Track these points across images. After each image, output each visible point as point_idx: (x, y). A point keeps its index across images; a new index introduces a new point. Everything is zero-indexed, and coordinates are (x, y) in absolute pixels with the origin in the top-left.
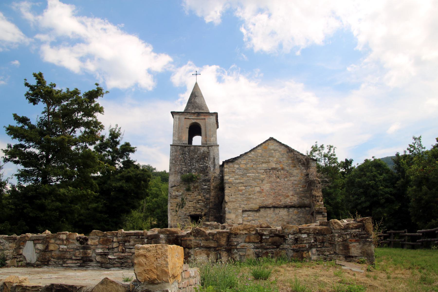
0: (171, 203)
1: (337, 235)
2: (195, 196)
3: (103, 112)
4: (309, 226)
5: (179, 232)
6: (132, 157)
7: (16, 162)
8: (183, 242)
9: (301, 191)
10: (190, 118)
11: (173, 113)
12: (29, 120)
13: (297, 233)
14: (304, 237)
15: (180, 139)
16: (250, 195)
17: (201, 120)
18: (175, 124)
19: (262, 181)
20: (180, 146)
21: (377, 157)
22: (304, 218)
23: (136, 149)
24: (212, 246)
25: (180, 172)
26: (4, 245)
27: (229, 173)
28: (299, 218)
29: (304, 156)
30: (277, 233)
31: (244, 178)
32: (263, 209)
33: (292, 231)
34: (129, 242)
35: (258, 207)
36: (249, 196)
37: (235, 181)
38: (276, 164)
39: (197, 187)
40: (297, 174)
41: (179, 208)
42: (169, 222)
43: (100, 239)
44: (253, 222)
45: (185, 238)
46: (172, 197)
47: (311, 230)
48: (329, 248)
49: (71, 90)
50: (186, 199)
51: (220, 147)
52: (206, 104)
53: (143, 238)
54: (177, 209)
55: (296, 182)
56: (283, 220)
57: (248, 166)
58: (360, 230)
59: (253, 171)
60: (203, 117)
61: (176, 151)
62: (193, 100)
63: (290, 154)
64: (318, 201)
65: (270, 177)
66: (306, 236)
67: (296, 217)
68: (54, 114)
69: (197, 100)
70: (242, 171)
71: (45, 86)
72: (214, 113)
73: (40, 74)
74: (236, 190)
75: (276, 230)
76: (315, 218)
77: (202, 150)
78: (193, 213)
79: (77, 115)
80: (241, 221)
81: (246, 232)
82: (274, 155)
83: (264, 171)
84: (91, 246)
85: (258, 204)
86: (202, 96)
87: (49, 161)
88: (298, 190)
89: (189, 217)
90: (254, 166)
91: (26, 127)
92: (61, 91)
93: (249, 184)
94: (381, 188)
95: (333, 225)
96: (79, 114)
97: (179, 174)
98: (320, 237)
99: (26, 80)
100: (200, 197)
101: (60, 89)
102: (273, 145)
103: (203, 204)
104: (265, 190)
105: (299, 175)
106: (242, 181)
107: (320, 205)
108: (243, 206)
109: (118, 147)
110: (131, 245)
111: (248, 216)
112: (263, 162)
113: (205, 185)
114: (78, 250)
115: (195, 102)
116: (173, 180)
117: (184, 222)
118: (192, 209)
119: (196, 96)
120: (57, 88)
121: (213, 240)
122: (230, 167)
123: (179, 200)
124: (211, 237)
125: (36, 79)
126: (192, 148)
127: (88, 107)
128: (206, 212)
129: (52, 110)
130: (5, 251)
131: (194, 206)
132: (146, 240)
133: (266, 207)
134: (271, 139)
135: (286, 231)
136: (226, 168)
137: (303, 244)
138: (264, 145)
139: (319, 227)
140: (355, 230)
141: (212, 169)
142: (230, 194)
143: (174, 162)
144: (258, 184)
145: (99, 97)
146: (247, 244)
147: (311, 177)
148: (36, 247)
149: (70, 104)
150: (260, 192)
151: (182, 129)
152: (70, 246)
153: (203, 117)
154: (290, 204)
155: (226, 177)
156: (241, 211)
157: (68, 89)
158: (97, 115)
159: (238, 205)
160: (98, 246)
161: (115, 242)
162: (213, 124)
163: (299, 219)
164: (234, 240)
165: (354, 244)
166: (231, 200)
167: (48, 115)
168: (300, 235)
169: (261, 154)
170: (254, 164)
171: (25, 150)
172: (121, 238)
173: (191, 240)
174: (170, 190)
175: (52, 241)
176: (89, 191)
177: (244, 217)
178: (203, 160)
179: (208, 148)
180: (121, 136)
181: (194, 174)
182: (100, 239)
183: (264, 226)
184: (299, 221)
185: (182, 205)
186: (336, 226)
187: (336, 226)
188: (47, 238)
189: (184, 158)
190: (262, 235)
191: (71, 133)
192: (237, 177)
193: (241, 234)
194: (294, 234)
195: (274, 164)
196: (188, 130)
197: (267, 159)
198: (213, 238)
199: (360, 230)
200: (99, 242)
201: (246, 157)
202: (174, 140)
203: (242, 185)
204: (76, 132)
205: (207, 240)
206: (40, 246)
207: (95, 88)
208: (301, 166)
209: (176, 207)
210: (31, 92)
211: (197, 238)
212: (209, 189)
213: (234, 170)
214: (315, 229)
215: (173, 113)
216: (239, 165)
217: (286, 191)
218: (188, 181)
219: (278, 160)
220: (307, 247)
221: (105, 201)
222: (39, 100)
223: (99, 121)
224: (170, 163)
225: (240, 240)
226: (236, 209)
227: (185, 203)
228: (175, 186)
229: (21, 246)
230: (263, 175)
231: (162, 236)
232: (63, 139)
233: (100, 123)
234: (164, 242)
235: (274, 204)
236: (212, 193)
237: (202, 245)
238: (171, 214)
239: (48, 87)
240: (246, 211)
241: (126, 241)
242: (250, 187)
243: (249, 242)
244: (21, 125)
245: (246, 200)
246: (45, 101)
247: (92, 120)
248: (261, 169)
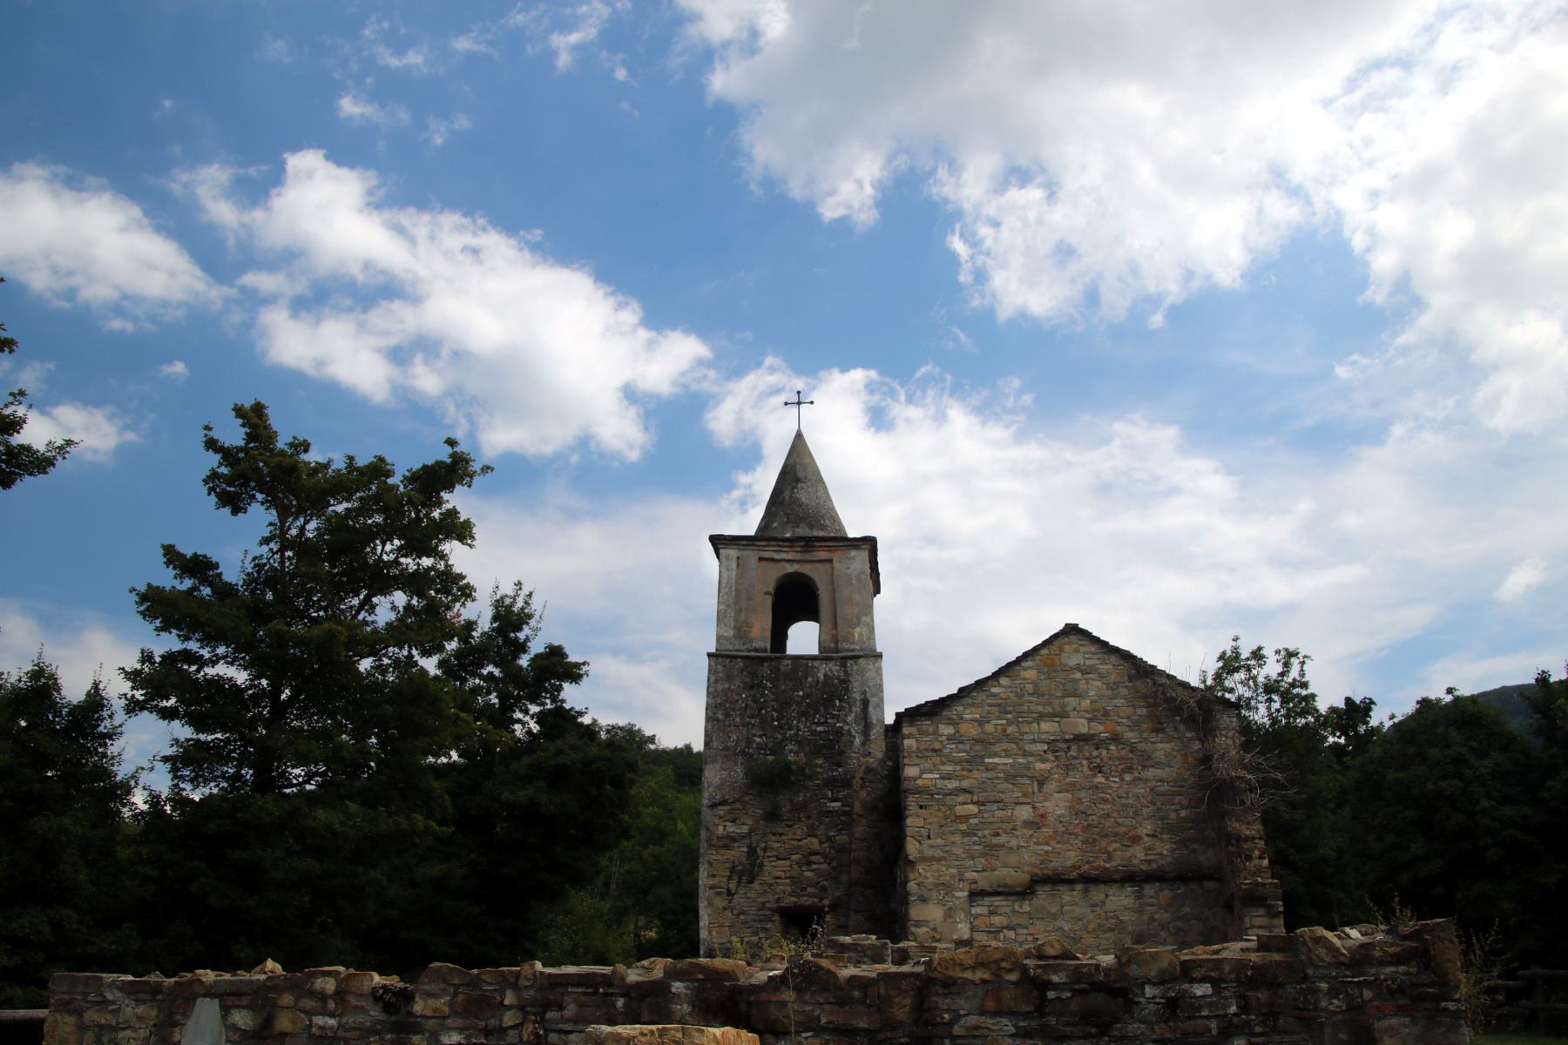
0: (710, 864)
1: (1324, 986)
2: (799, 837)
3: (472, 538)
4: (1217, 952)
5: (740, 975)
6: (572, 696)
7: (168, 714)
8: (754, 1011)
10: (776, 556)
11: (718, 542)
12: (216, 566)
13: (1175, 979)
14: (1199, 993)
15: (741, 632)
17: (819, 566)
18: (725, 581)
19: (1041, 784)
20: (743, 658)
21: (1465, 691)
23: (585, 668)
24: (863, 1025)
25: (743, 753)
26: (117, 1011)
27: (920, 753)
28: (1179, 918)
29: (1195, 689)
30: (1101, 977)
31: (976, 774)
33: (1154, 973)
34: (561, 1008)
35: (1028, 877)
36: (995, 840)
37: (940, 783)
38: (1090, 720)
39: (803, 806)
40: (1168, 755)
41: (739, 882)
42: (703, 934)
43: (456, 994)
44: (1011, 934)
45: (764, 996)
46: (715, 842)
47: (1227, 968)
48: (1295, 1037)
49: (363, 461)
50: (765, 849)
51: (885, 664)
52: (833, 509)
53: (612, 995)
54: (733, 886)
55: (1165, 787)
56: (1120, 927)
57: (989, 728)
58: (1413, 970)
59: (1005, 746)
60: (823, 555)
61: (729, 678)
62: (787, 494)
63: (1139, 684)
64: (1249, 858)
65: (1068, 768)
66: (1210, 991)
67: (1167, 916)
68: (301, 546)
69: (803, 496)
70: (968, 747)
71: (272, 450)
73: (259, 409)
74: (946, 817)
75: (1097, 966)
76: (1241, 918)
77: (823, 670)
78: (789, 901)
79: (379, 548)
80: (963, 931)
81: (986, 976)
82: (1082, 686)
84: (423, 1021)
85: (1027, 868)
86: (820, 481)
87: (279, 709)
88: (1173, 816)
89: (776, 917)
90: (1010, 730)
91: (206, 591)
92: (326, 466)
93: (993, 795)
94: (1486, 804)
95: (1310, 951)
96: (388, 547)
98: (1262, 995)
99: (208, 428)
100: (814, 840)
101: (322, 460)
102: (1076, 651)
103: (824, 866)
104: (1050, 818)
105: (1178, 762)
106: (965, 784)
107: (1258, 869)
108: (970, 875)
109: (524, 661)
110: (568, 1020)
111: (992, 913)
112: (1042, 716)
113: (834, 800)
114: (376, 1032)
115: (797, 502)
116: (717, 781)
117: (756, 934)
118: (784, 886)
119: (798, 480)
120: (313, 457)
121: (862, 1002)
122: (921, 732)
123: (739, 852)
124: (856, 994)
125: (243, 425)
126: (785, 666)
127: (419, 520)
129: (294, 532)
130: (122, 1034)
131: (794, 873)
132: (620, 1003)
133: (1056, 880)
134: (1071, 630)
135: (1134, 971)
136: (910, 736)
137: (1199, 1022)
138: (1044, 651)
139: (1253, 957)
140: (1392, 969)
141: (858, 741)
143: (720, 716)
144: (1025, 795)
145: (458, 487)
146: (989, 1021)
147: (1223, 770)
148: (230, 1021)
149: (356, 509)
150: (1028, 824)
151: (749, 599)
152: (350, 1020)
153: (823, 555)
154: (1143, 867)
155: (910, 771)
156: (966, 894)
157: (351, 458)
158: (452, 548)
159: (954, 871)
160: (449, 1021)
161: (510, 1007)
162: (859, 580)
163: (1179, 924)
164: (944, 1003)
165: (1394, 1021)
166: (929, 853)
167: (282, 550)
168: (1185, 986)
169: (1035, 684)
170: (1010, 723)
171: (198, 671)
172: (532, 993)
173: (783, 1004)
174: (707, 815)
175: (287, 999)
176: (419, 817)
177: (977, 916)
179: (844, 665)
180: (533, 622)
181: (791, 757)
182: (456, 994)
183: (1050, 951)
184: (1179, 930)
185: (748, 872)
186: (1321, 951)
187: (1321, 951)
188: (269, 989)
189: (756, 701)
190: (1049, 985)
191: (358, 612)
192: (948, 768)
193: (966, 982)
194: (1162, 982)
196: (769, 600)
197: (1056, 703)
198: (866, 995)
199: (1413, 970)
200: (451, 1004)
201: (980, 696)
202: (719, 638)
203: (968, 796)
204: (378, 610)
205: (841, 1005)
206: (242, 1018)
207: (444, 454)
208: (1182, 727)
209: (730, 878)
210: (224, 470)
211: (808, 997)
213: (937, 746)
214: (1240, 965)
215: (718, 542)
216: (955, 724)
217: (1128, 821)
218: (770, 784)
220: (1214, 1032)
221: (473, 856)
222: (253, 497)
223: (457, 569)
224: (708, 719)
225: (962, 1004)
226: (947, 888)
227: (761, 866)
228: (723, 802)
229: (178, 1017)
230: (1044, 761)
231: (678, 987)
232: (332, 635)
233: (462, 577)
234: (686, 1008)
235: (1086, 867)
236: (860, 829)
237: (824, 1020)
238: (710, 904)
239: (282, 453)
240: (983, 893)
241: (547, 1006)
242: (995, 807)
243: (996, 1013)
244: (188, 583)
245: (983, 855)
246: (272, 502)
247: (433, 568)
248: (1034, 741)
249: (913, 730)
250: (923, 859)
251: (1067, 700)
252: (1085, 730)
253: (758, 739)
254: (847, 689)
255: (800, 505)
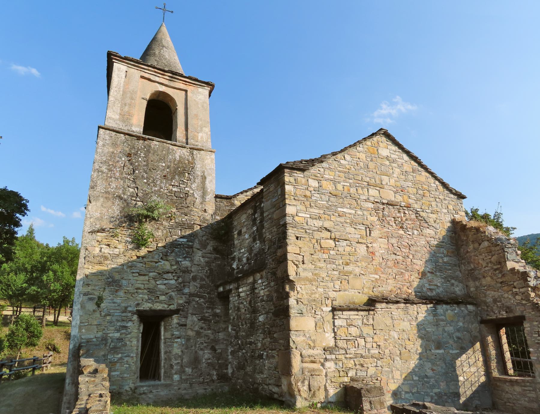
9: (445, 263)
10: (152, 77)
16: (347, 264)
22: (468, 332)
28: (458, 330)
32: (384, 305)
35: (365, 299)
36: (347, 268)
38: (395, 193)
57: (340, 187)
60: (181, 85)
61: (114, 145)
72: (208, 84)
78: (146, 306)
83: (372, 206)
85: (366, 290)
89: (135, 317)
97: (117, 202)
100: (167, 263)
106: (327, 224)
108: (332, 294)
117: (118, 331)
128: (179, 305)
131: (151, 286)
141: (198, 201)
142: (300, 258)
143: (104, 169)
151: (132, 99)
153: (181, 85)
154: (429, 294)
178: (179, 175)
184: (459, 338)
195: (393, 193)
196: (145, 103)
212: (191, 247)
213: (308, 193)
219: (398, 184)
238: (83, 307)
249: (292, 179)
250: (300, 279)
251: (382, 176)
252: (393, 199)
253: (131, 190)
254: (193, 168)
255: (165, 59)
